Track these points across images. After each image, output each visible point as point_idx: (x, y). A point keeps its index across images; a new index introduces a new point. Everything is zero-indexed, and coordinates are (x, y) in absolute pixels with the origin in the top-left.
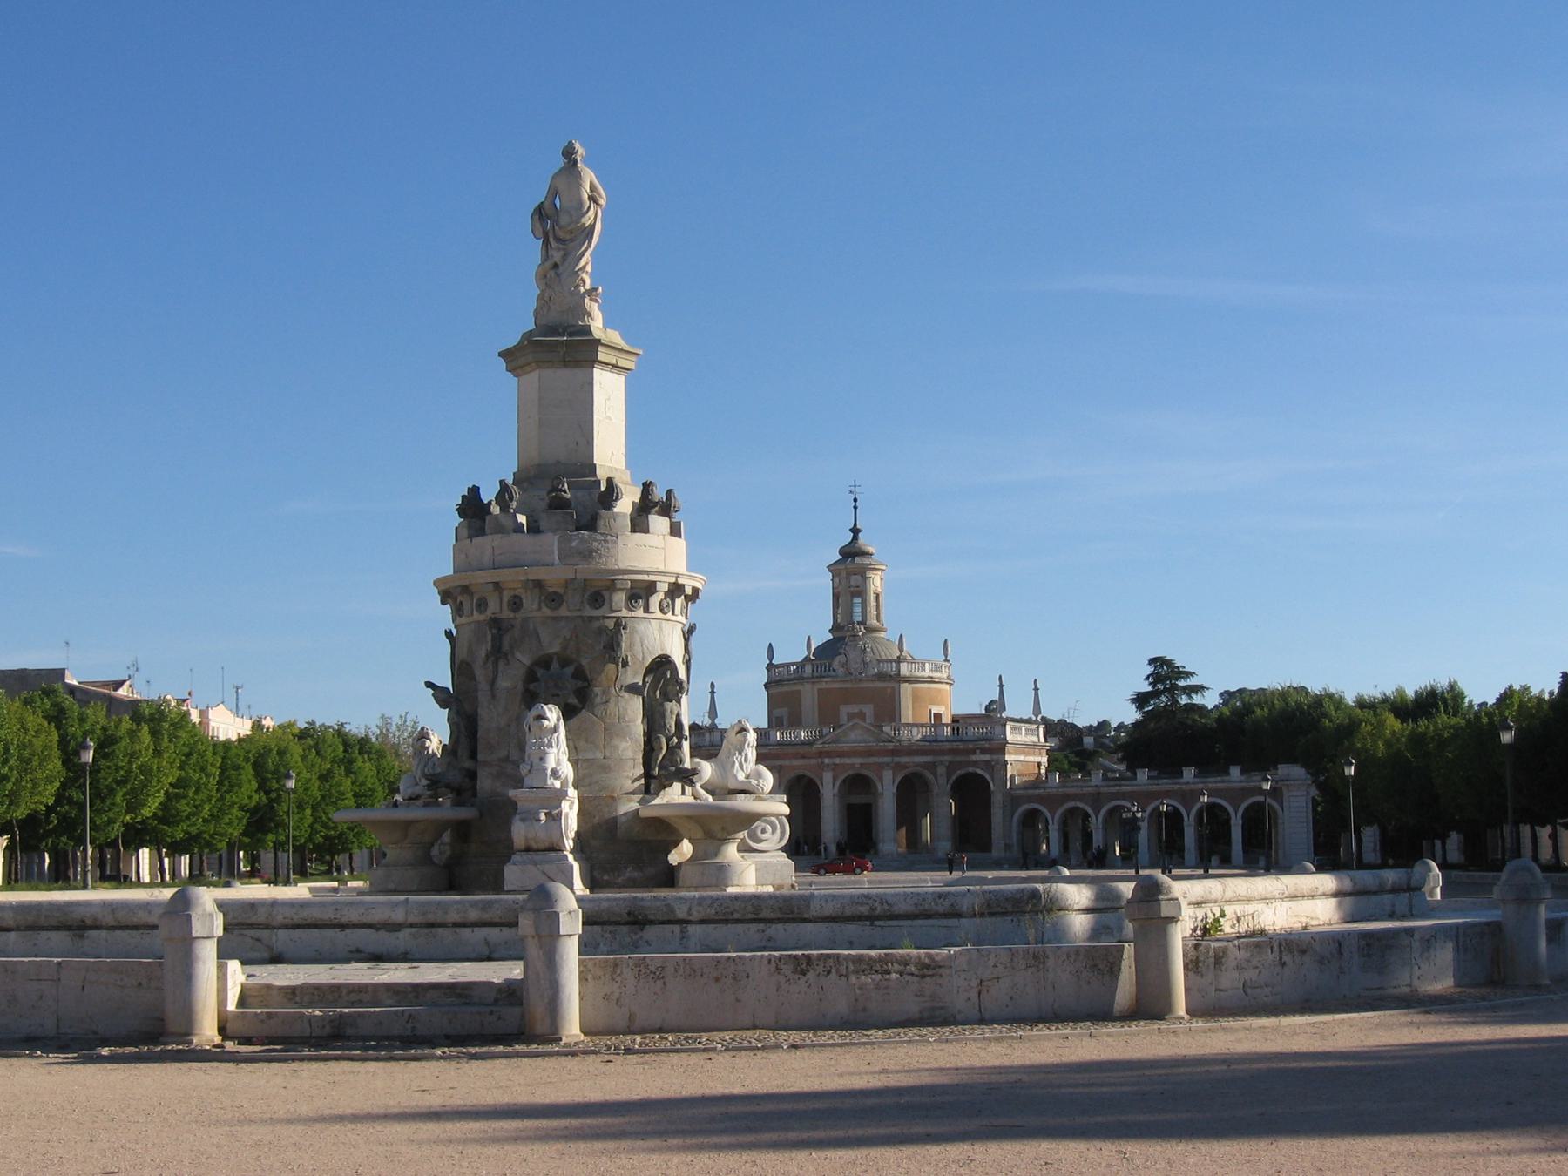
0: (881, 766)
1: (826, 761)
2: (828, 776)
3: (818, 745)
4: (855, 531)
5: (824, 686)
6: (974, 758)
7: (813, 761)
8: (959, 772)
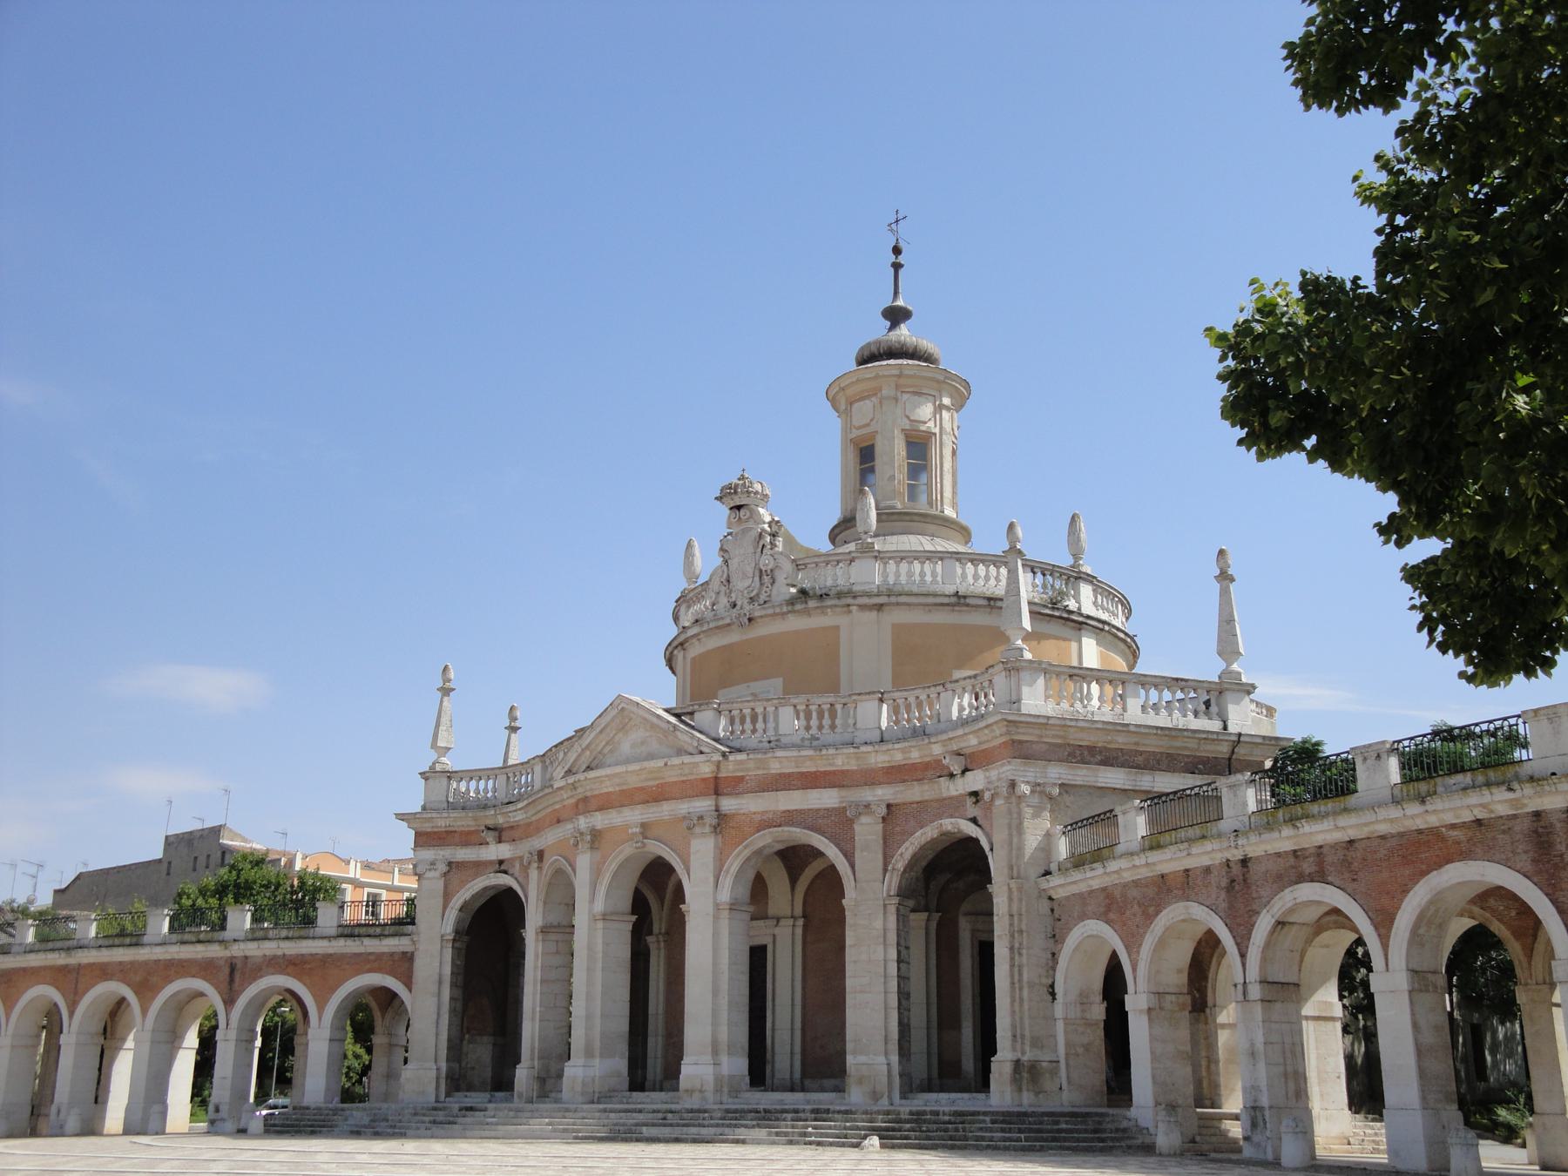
0: (691, 824)
5: (695, 650)
8: (926, 834)
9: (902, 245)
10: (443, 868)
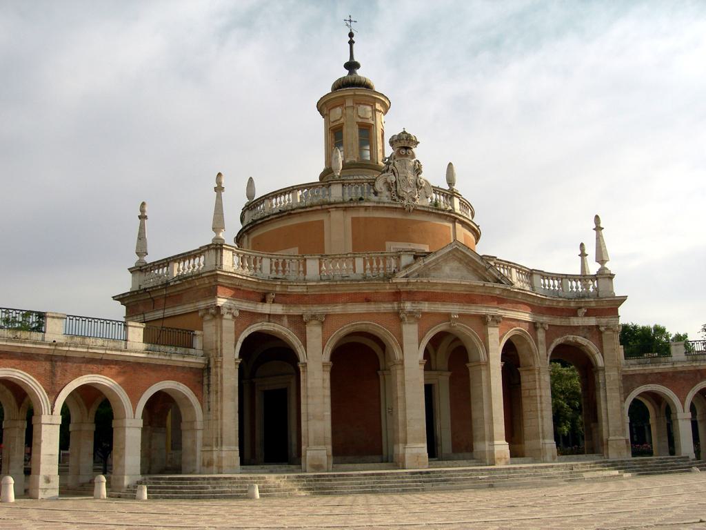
0: (483, 320)
1: (408, 306)
2: (410, 331)
3: (400, 279)
4: (352, 66)
5: (362, 214)
6: (575, 321)
7: (387, 307)
8: (558, 341)
9: (353, 31)
10: (237, 313)
